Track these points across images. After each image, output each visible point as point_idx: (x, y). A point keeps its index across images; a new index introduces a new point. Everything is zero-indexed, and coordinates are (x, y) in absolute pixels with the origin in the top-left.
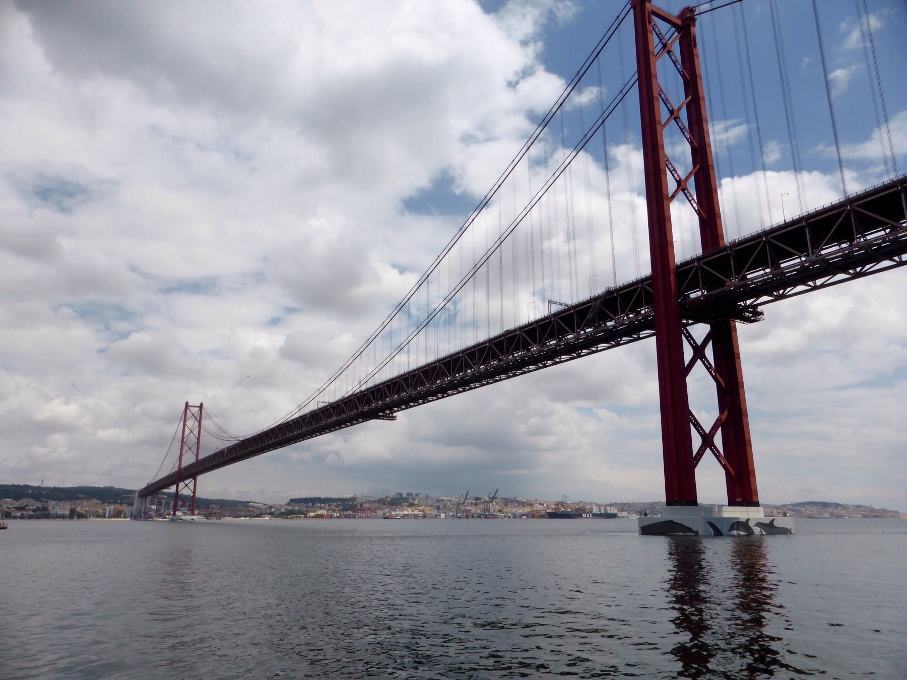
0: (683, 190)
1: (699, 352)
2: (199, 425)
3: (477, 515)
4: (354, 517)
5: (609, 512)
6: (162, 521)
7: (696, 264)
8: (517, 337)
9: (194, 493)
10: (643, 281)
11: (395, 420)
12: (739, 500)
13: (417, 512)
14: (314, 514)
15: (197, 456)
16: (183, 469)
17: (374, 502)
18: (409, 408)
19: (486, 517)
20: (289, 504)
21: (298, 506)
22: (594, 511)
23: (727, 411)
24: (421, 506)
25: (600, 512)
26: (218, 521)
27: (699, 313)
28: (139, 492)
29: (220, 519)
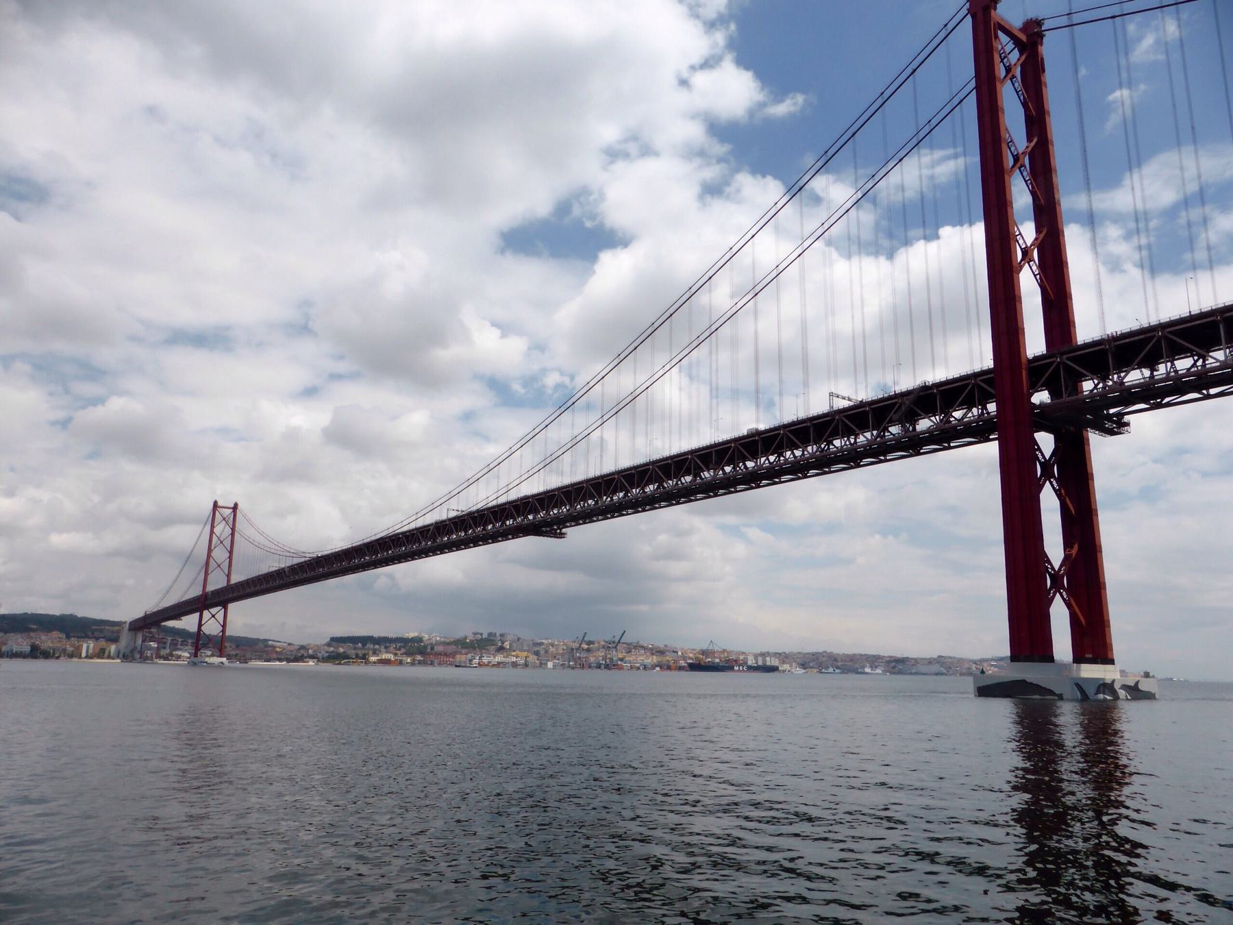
2: (232, 534)
3: (595, 665)
4: (431, 664)
5: (768, 664)
6: (174, 665)
7: (1058, 360)
8: (780, 437)
9: (224, 626)
11: (562, 538)
12: (1089, 656)
16: (210, 593)
19: (607, 667)
20: (329, 645)
21: (343, 647)
22: (750, 663)
23: (1077, 544)
24: (514, 651)
25: (757, 663)
26: (243, 665)
27: (1044, 418)
28: (131, 623)
29: (247, 663)
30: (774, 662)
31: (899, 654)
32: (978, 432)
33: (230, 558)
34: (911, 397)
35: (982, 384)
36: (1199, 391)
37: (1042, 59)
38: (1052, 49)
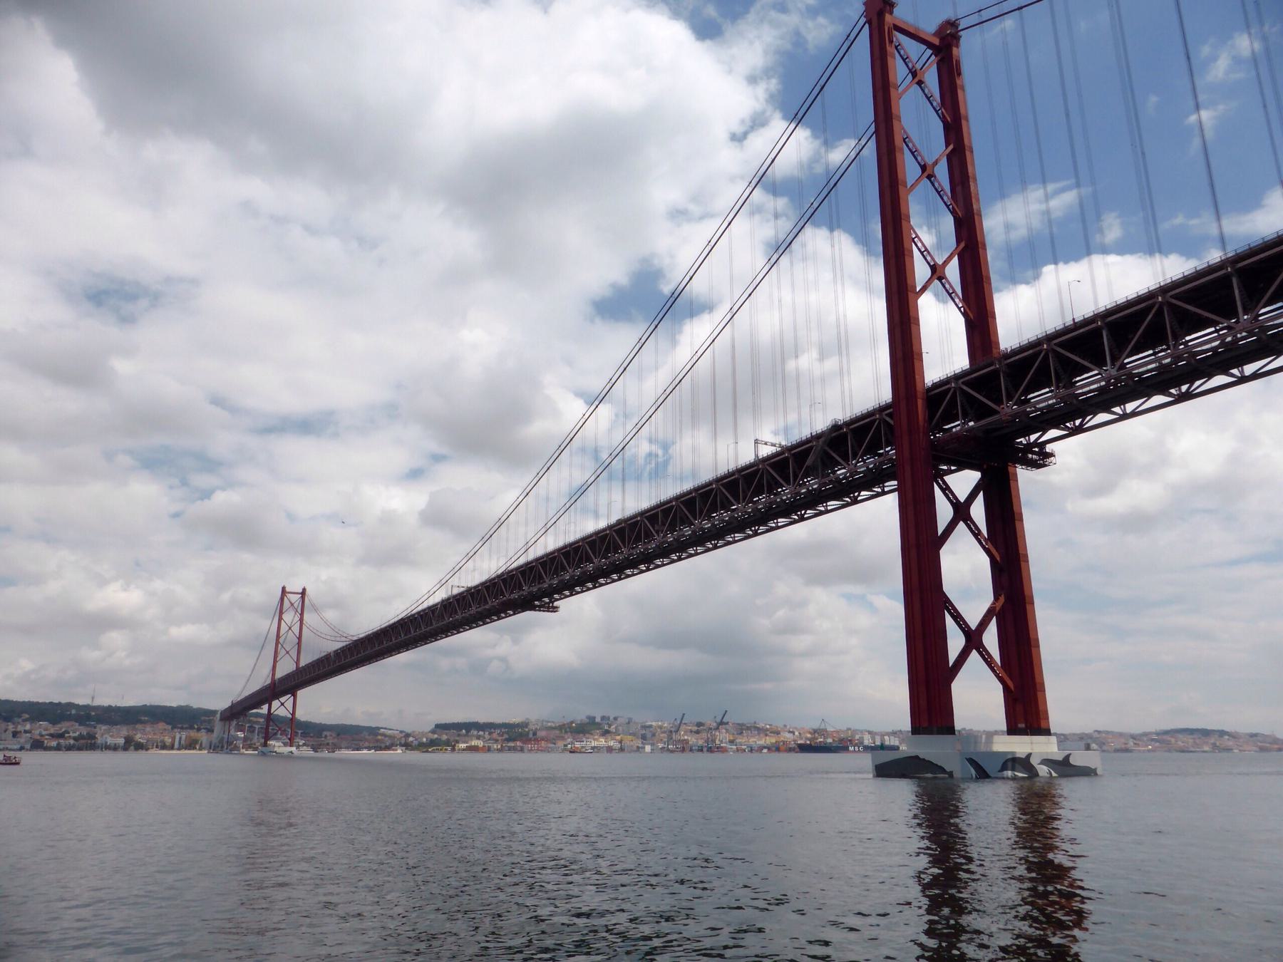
0: (940, 279)
1: (961, 511)
3: (697, 748)
5: (887, 743)
7: (953, 385)
9: (293, 714)
10: (882, 409)
11: (557, 611)
12: (1022, 726)
13: (611, 743)
14: (465, 745)
15: (297, 662)
17: (554, 728)
18: (575, 595)
19: (710, 750)
20: (433, 732)
21: (446, 734)
22: (866, 742)
23: (1003, 596)
24: (619, 735)
25: (874, 743)
26: (331, 755)
29: (334, 752)
34: (822, 439)
37: (958, 62)
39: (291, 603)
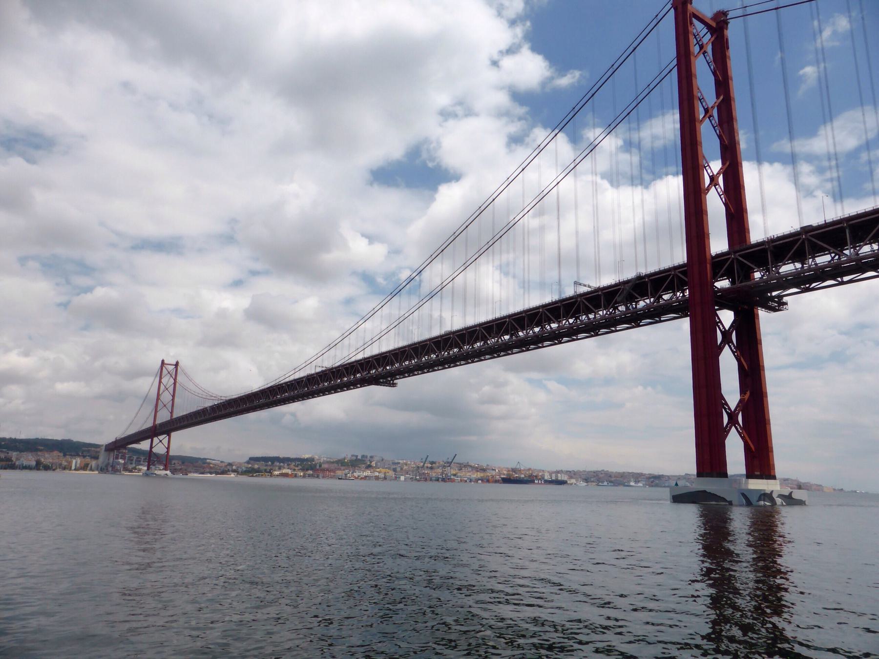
3: (435, 479)
5: (559, 479)
6: (136, 475)
7: (733, 256)
8: (540, 314)
9: (168, 448)
12: (758, 473)
14: (279, 472)
15: (172, 413)
16: (158, 425)
17: (333, 463)
19: (443, 480)
20: (248, 462)
24: (379, 468)
25: (551, 478)
27: (725, 300)
28: (106, 445)
29: (187, 475)
30: (564, 477)
31: (656, 472)
32: (679, 310)
33: (173, 400)
34: (630, 284)
35: (680, 275)
36: (834, 279)
37: (727, 40)
38: (733, 32)
39: (168, 371)
